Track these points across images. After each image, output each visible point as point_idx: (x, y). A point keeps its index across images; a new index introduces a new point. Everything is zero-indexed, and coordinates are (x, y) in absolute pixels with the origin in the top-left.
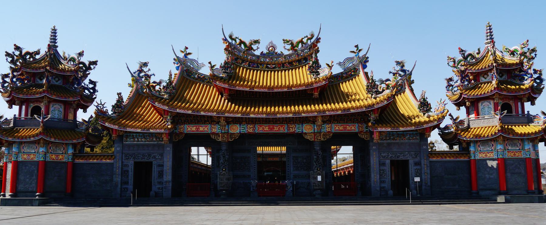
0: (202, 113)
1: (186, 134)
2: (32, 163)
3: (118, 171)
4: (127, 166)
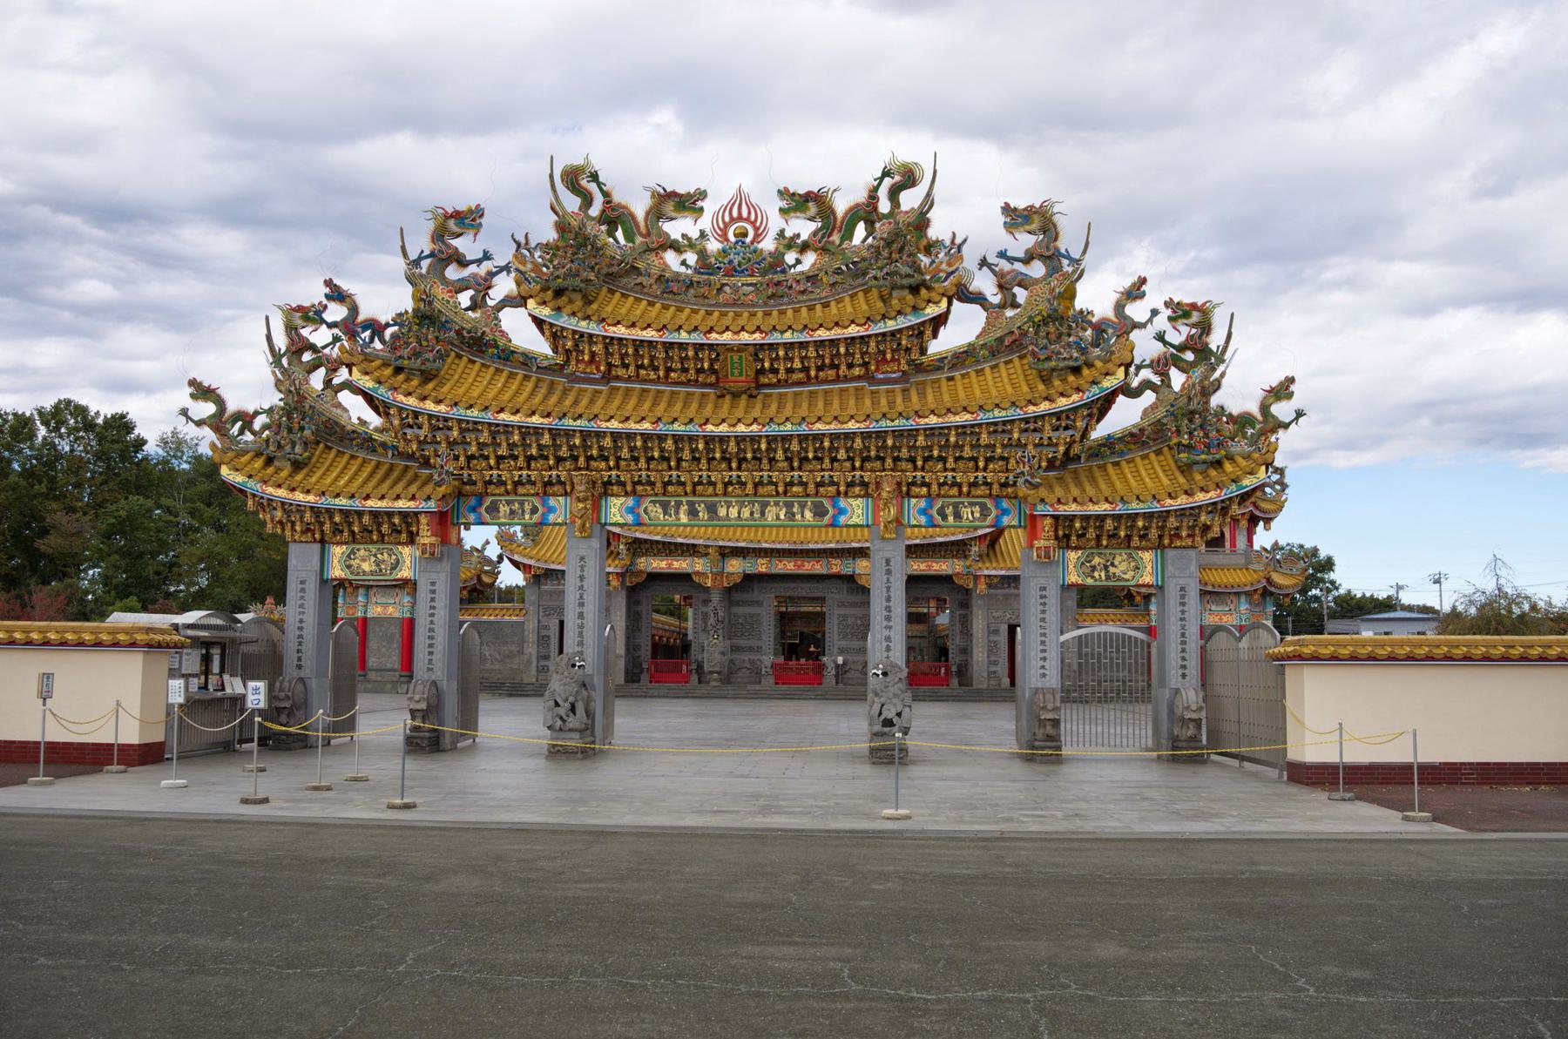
0: (680, 540)
1: (650, 575)
2: (391, 619)
3: (531, 637)
4: (546, 627)
